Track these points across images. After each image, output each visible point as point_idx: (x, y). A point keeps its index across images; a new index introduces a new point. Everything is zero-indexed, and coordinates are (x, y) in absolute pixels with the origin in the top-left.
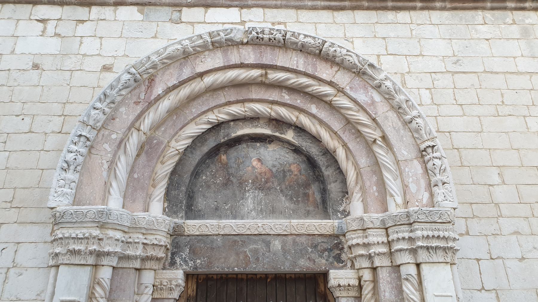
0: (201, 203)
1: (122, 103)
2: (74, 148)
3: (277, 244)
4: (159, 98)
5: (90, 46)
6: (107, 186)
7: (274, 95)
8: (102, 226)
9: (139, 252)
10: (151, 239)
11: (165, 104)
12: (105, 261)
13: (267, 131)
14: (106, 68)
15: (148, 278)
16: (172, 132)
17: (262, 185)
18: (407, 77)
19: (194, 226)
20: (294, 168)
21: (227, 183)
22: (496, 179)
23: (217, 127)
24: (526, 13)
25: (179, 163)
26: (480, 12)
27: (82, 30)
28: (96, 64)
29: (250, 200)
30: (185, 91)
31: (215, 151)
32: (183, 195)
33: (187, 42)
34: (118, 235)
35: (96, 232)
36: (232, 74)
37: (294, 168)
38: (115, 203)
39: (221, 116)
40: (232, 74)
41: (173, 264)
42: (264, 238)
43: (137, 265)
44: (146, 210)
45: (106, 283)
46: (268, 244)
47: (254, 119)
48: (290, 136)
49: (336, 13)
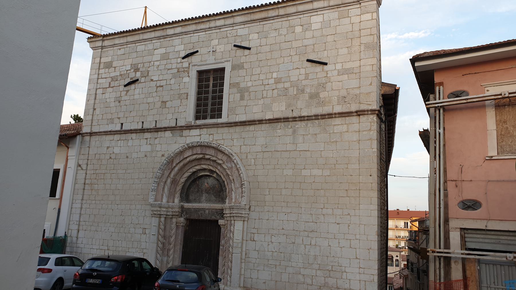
0: (191, 198)
1: (165, 169)
2: (154, 185)
3: (207, 211)
4: (175, 167)
5: (158, 148)
6: (162, 195)
7: (208, 162)
8: (160, 207)
9: (171, 214)
10: (174, 210)
11: (176, 169)
12: (162, 216)
13: (208, 174)
14: (163, 155)
15: (174, 220)
16: (180, 176)
17: (207, 191)
18: (248, 154)
19: (187, 205)
20: (217, 186)
21: (198, 191)
22: (268, 193)
23: (194, 173)
24: (297, 122)
25: (183, 186)
26: (280, 124)
27: (157, 141)
28: (159, 154)
29: (204, 197)
30: (182, 164)
31: (195, 181)
32: (185, 196)
33: (180, 148)
34: (164, 209)
35: (159, 209)
36: (194, 157)
37: (217, 186)
38: (165, 200)
39: (194, 170)
40: (194, 157)
41: (181, 216)
42: (204, 209)
43: (171, 217)
44: (174, 202)
45: (163, 222)
46: (205, 211)
47: (204, 170)
48: (215, 175)
49: (230, 128)
